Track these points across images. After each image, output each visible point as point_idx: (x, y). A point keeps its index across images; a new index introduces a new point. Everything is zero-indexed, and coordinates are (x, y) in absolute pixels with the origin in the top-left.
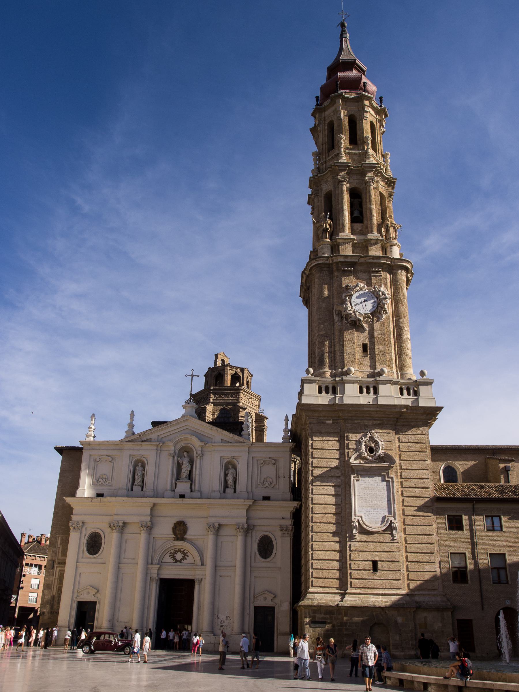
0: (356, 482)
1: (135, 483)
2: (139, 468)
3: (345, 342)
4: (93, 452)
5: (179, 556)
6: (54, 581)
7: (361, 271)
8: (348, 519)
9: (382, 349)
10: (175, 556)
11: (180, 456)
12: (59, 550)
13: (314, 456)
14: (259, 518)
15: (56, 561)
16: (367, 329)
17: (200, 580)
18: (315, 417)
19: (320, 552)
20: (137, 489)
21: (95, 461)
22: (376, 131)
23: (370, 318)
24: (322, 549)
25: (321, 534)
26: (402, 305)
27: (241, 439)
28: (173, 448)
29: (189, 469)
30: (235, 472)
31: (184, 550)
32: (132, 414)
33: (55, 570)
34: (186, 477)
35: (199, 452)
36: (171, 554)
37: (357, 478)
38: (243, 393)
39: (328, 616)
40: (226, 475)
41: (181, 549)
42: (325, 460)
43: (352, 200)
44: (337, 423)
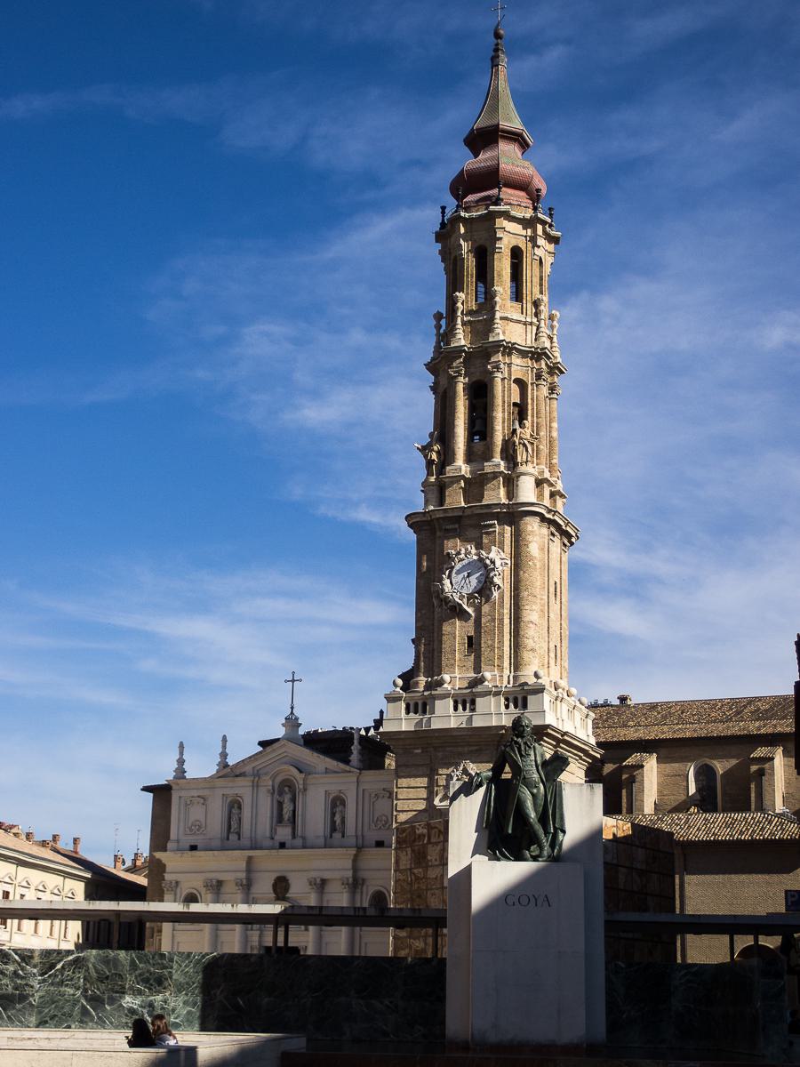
1: (232, 830)
2: (235, 811)
3: (444, 637)
4: (183, 793)
7: (471, 526)
9: (490, 642)
11: (281, 793)
13: (399, 797)
14: (369, 870)
15: (155, 930)
16: (473, 615)
20: (233, 837)
21: (186, 805)
22: (525, 259)
23: (477, 599)
26: (524, 572)
27: (348, 768)
28: (270, 783)
29: (292, 808)
32: (224, 739)
34: (288, 820)
35: (301, 787)
40: (333, 814)
43: (474, 401)
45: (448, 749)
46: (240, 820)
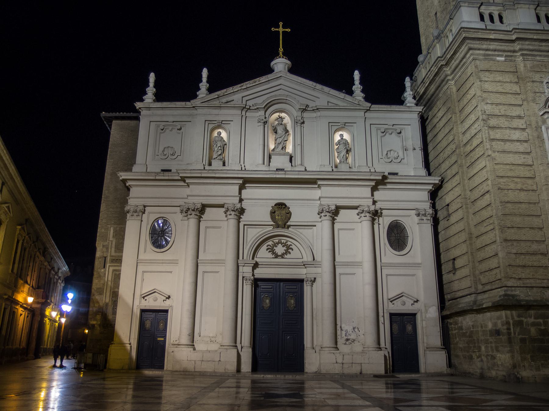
1: (214, 157)
5: (280, 249)
6: (106, 284)
10: (275, 250)
12: (112, 244)
15: (108, 259)
17: (313, 279)
18: (481, 52)
19: (513, 231)
24: (515, 226)
25: (509, 205)
31: (286, 242)
33: (107, 270)
39: (541, 321)
41: (283, 241)
44: (511, 61)
45: (538, 58)
46: (224, 148)
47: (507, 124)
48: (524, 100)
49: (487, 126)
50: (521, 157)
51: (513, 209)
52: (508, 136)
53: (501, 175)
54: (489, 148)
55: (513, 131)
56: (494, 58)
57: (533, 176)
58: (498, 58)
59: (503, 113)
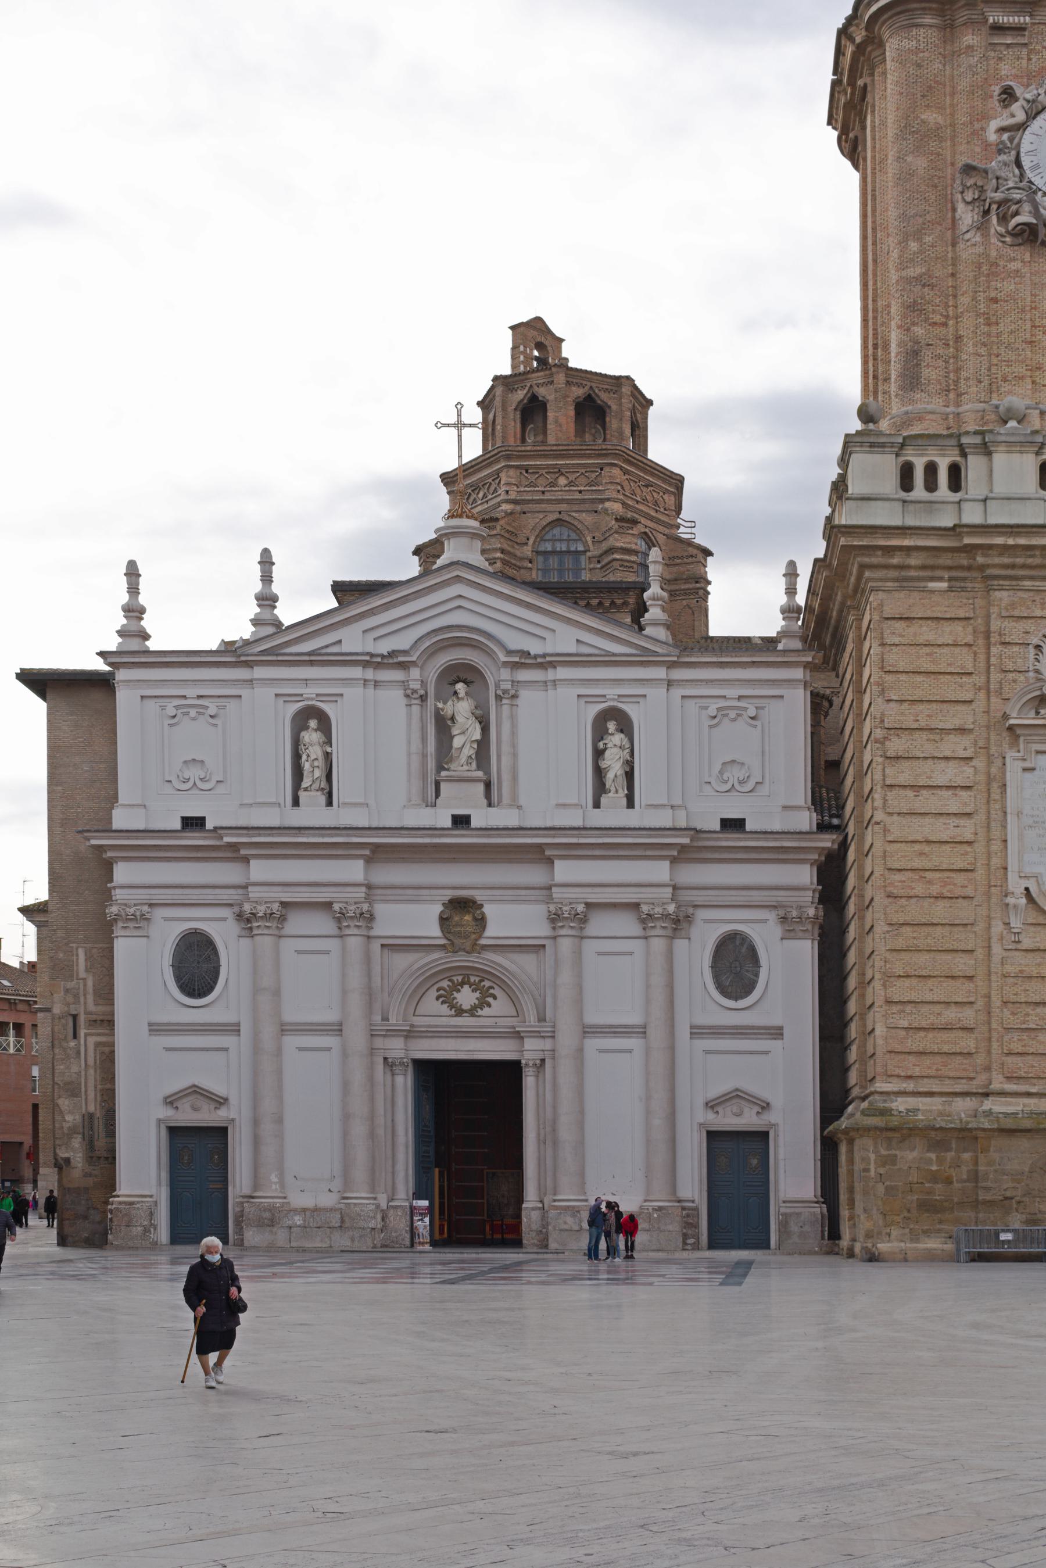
0: (1028, 775)
5: (466, 997)
8: (995, 886)
10: (455, 998)
25: (907, 930)
30: (626, 743)
31: (481, 981)
36: (442, 992)
37: (1027, 765)
38: (621, 468)
42: (921, 707)
44: (963, 589)
45: (1027, 583)
47: (930, 749)
48: (980, 689)
49: (881, 756)
50: (949, 824)
51: (914, 938)
52: (927, 778)
53: (896, 865)
54: (881, 806)
55: (943, 764)
56: (922, 584)
57: (969, 867)
58: (932, 585)
59: (922, 724)
